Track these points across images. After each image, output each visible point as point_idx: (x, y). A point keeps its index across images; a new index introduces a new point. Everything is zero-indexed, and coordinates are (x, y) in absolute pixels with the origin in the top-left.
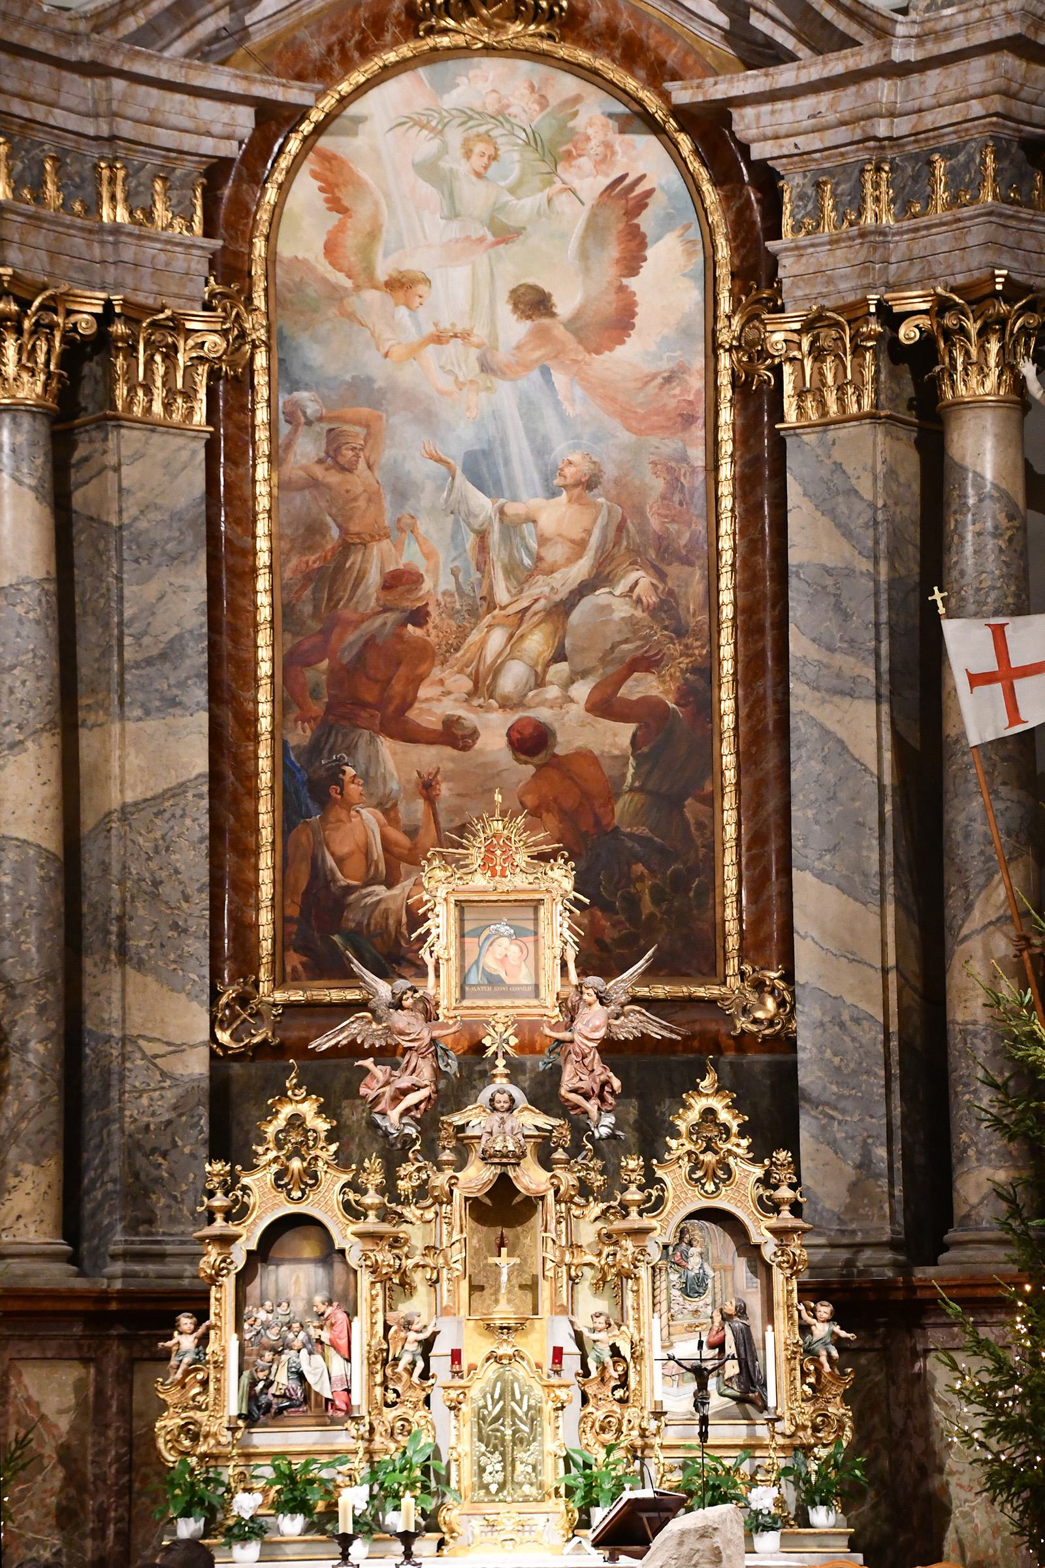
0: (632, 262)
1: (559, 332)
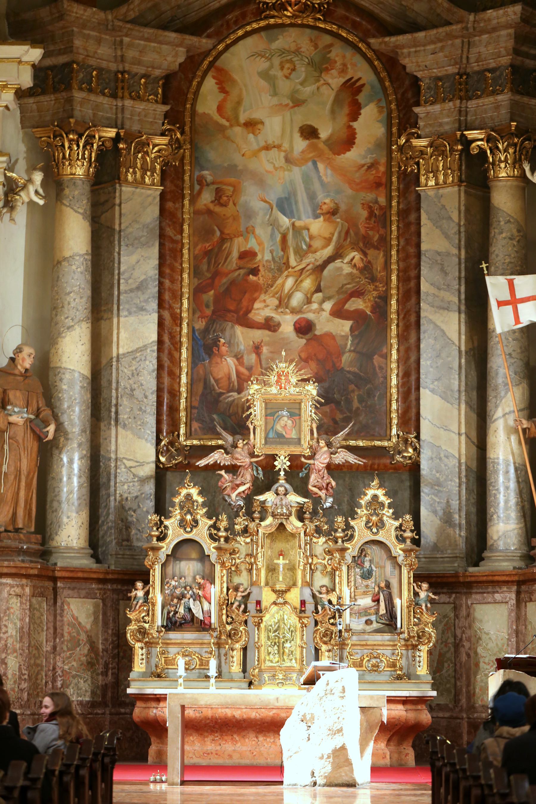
0: (354, 115)
1: (321, 145)
